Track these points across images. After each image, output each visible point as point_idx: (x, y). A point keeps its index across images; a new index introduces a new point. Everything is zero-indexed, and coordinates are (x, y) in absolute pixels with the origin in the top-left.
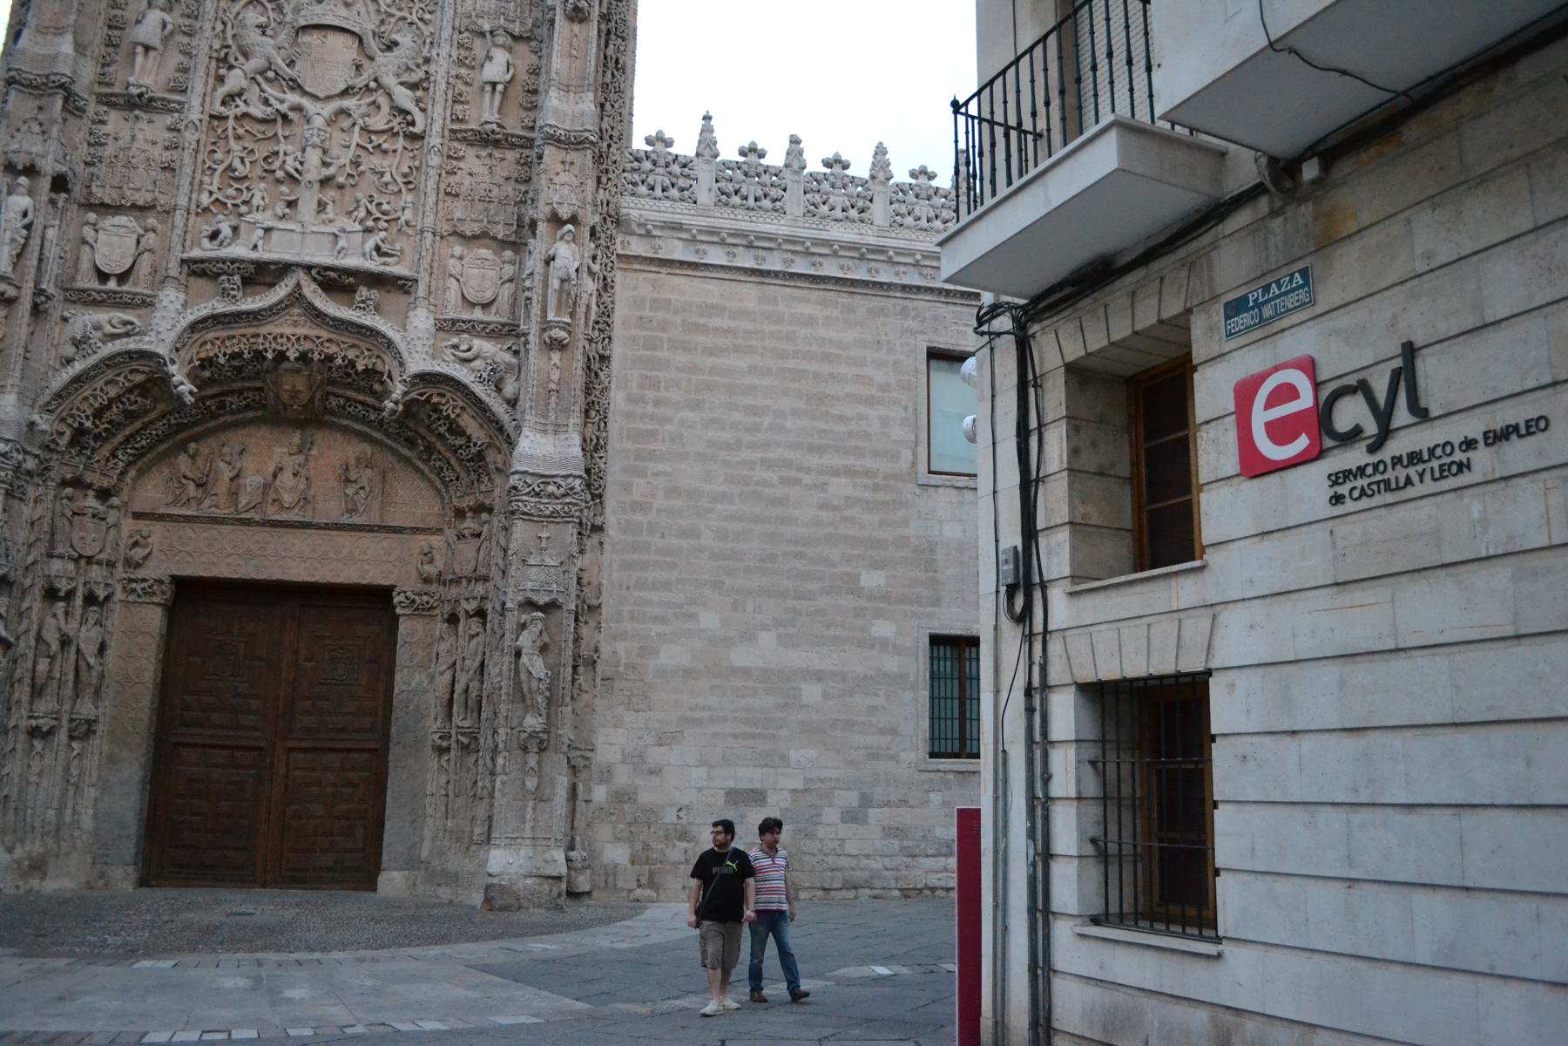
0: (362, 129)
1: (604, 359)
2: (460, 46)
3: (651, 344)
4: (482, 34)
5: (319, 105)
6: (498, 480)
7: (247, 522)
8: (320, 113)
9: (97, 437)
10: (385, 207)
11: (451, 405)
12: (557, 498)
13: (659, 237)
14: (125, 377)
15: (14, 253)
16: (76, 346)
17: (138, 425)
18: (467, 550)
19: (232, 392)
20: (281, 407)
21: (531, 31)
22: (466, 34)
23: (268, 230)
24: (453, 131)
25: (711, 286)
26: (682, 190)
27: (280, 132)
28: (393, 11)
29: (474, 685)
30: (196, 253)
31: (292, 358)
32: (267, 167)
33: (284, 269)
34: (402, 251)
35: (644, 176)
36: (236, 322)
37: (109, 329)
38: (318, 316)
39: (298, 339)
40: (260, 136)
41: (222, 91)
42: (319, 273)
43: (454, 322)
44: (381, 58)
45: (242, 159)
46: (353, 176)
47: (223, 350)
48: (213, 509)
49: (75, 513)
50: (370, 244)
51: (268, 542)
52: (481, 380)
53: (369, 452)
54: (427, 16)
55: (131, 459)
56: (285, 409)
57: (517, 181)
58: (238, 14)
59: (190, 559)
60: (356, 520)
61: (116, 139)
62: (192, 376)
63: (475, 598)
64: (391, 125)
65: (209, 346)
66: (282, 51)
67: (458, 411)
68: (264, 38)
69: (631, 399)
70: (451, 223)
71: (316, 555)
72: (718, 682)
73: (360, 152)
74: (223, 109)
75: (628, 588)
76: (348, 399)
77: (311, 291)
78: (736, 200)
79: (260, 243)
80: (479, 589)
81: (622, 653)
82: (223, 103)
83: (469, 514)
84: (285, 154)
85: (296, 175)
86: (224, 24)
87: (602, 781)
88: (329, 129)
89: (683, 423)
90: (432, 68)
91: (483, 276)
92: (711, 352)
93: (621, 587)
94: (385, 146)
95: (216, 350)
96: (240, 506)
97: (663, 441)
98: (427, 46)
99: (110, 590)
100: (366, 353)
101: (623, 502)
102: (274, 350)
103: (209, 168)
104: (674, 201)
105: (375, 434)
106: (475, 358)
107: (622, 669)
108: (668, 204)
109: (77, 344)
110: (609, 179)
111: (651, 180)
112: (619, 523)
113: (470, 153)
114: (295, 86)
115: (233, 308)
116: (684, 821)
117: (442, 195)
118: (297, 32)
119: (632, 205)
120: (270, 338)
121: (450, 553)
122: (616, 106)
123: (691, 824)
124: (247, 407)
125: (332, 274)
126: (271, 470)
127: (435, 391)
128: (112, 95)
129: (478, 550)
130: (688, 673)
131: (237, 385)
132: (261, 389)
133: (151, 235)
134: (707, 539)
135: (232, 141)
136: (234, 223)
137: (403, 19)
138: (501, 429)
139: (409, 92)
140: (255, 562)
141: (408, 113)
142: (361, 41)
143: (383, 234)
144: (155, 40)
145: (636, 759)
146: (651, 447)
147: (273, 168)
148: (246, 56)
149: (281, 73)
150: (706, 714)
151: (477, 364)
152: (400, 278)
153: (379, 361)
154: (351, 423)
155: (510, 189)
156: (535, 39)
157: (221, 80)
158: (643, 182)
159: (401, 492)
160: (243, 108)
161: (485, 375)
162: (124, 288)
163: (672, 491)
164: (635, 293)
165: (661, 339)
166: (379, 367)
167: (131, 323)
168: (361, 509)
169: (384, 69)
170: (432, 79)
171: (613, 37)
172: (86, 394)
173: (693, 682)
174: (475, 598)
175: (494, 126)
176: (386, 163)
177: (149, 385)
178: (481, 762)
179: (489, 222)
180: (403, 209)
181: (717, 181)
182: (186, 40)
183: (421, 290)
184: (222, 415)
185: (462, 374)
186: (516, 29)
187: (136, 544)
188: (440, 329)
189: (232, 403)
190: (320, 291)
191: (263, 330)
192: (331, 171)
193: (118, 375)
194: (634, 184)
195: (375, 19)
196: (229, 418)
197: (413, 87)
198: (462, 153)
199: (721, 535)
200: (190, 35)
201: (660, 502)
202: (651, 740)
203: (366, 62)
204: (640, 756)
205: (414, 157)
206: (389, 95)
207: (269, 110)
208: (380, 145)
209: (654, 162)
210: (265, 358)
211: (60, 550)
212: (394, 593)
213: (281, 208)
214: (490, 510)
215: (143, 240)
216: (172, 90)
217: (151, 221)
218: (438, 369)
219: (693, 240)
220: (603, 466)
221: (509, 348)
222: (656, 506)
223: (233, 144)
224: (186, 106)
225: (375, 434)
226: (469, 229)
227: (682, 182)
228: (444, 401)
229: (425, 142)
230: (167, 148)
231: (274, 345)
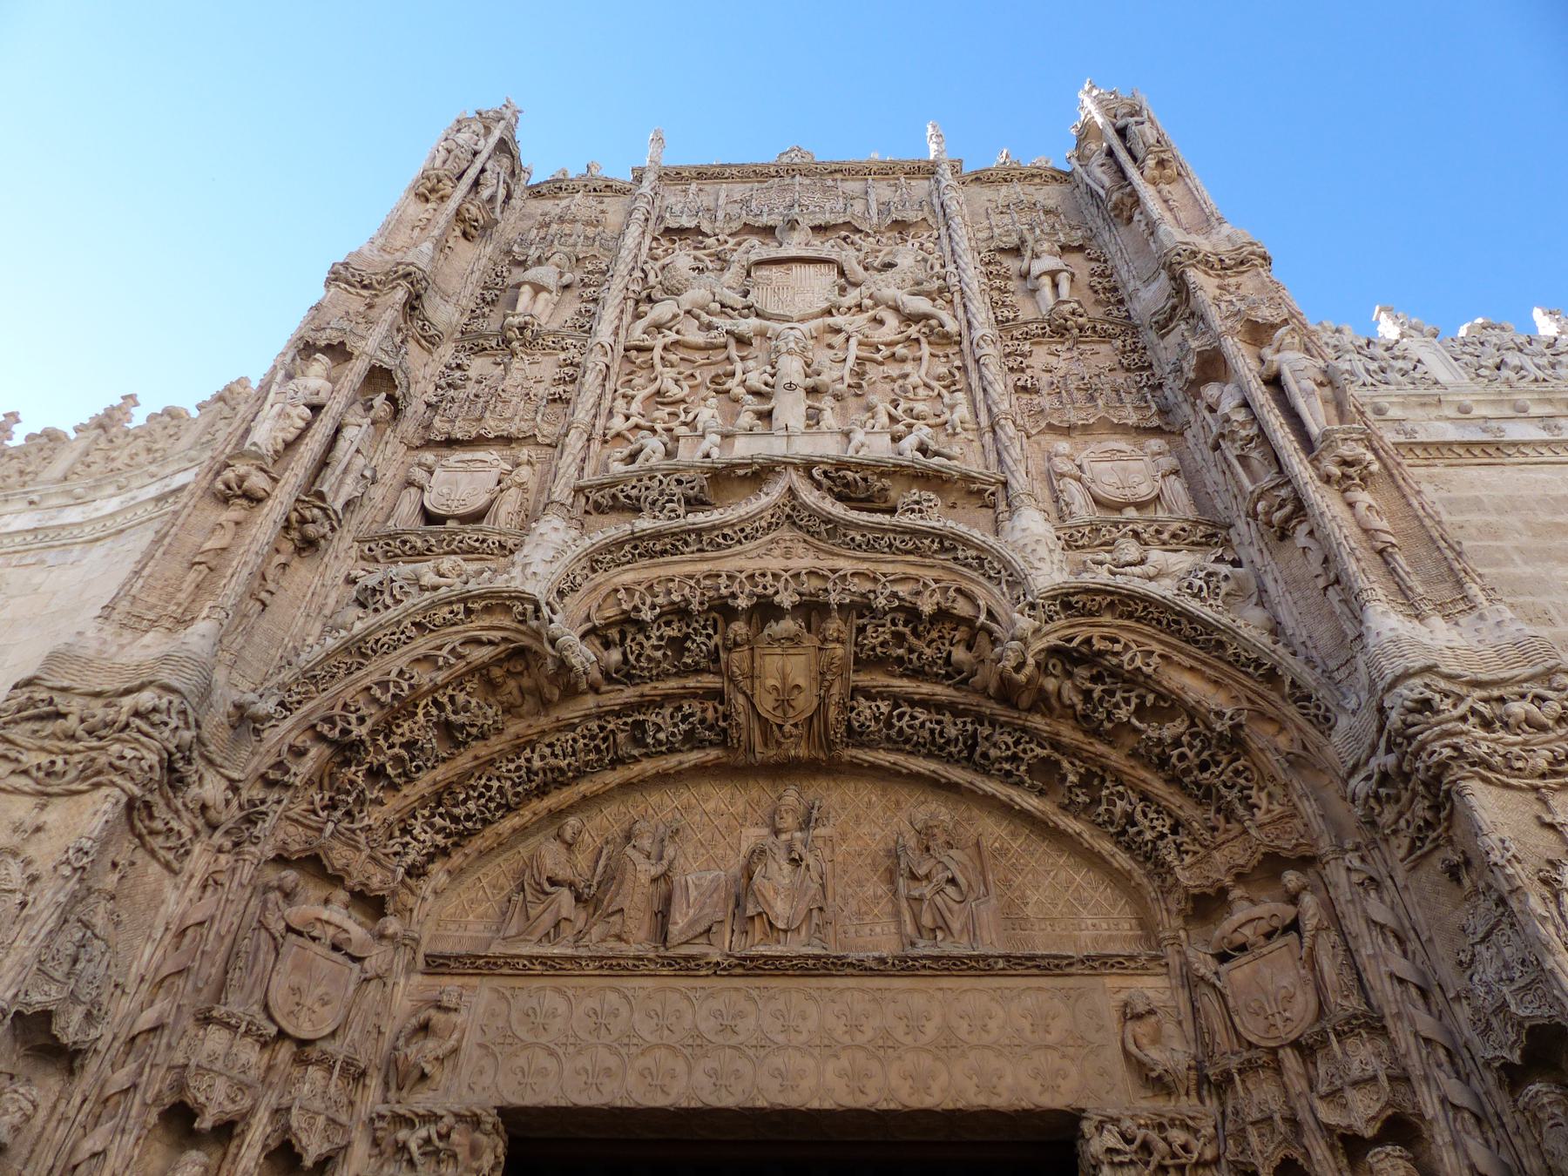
0: (860, 344)
7: (687, 966)
9: (376, 773)
12: (1543, 728)
15: (281, 435)
17: (464, 761)
20: (757, 737)
36: (676, 550)
42: (825, 473)
47: (649, 601)
48: (612, 943)
51: (741, 1015)
53: (947, 818)
55: (440, 839)
59: (551, 1064)
60: (948, 948)
67: (1155, 660)
71: (861, 1039)
76: (897, 700)
83: (1236, 893)
95: (637, 600)
99: (339, 1140)
100: (934, 586)
105: (958, 775)
121: (1209, 1002)
124: (692, 740)
127: (1096, 632)
129: (1312, 962)
131: (672, 685)
132: (717, 695)
138: (1272, 676)
140: (709, 1064)
154: (900, 759)
159: (1033, 897)
166: (962, 608)
168: (956, 926)
172: (367, 682)
184: (636, 760)
187: (425, 1028)
189: (659, 729)
193: (440, 648)
196: (649, 766)
212: (1087, 1127)
225: (958, 775)
228: (1118, 647)
229: (966, 344)
231: (747, 588)
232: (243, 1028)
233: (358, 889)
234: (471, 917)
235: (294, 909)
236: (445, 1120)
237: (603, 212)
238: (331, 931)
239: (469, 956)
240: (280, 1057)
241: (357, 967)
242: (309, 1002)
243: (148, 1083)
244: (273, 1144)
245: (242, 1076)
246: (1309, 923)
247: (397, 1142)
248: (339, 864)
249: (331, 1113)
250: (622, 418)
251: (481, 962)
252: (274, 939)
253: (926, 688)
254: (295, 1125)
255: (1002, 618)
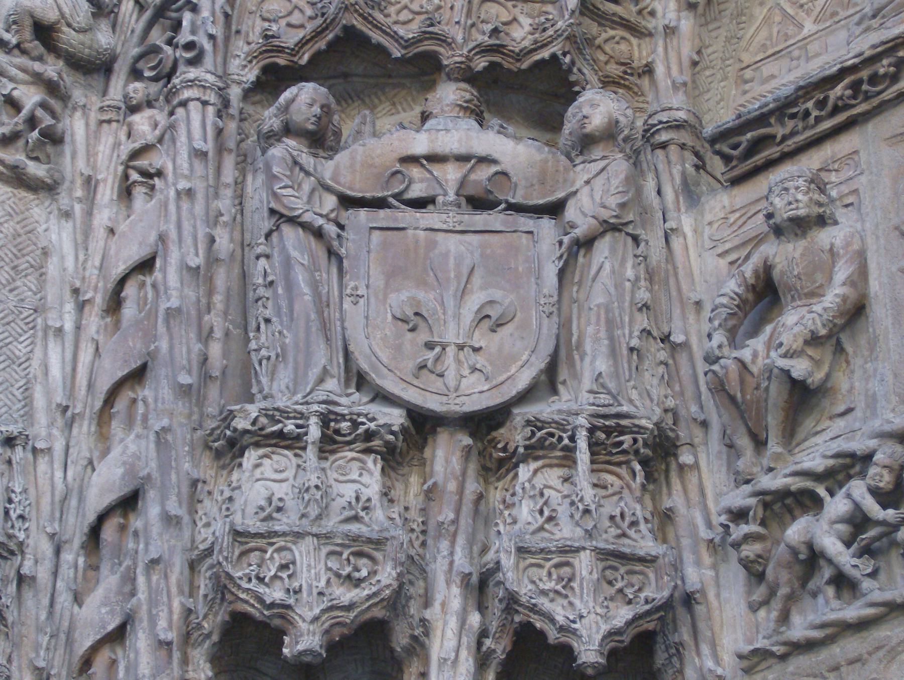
232: (314, 432)
233: (480, 64)
234: (809, 27)
235: (342, 157)
236: (878, 457)
238: (451, 174)
239: (807, 90)
240: (439, 467)
241: (546, 226)
242: (451, 335)
243: (153, 602)
244: (499, 647)
245: (354, 528)
247: (794, 551)
248: (408, 32)
249: (607, 540)
251: (839, 90)
252: (318, 234)
254: (524, 590)
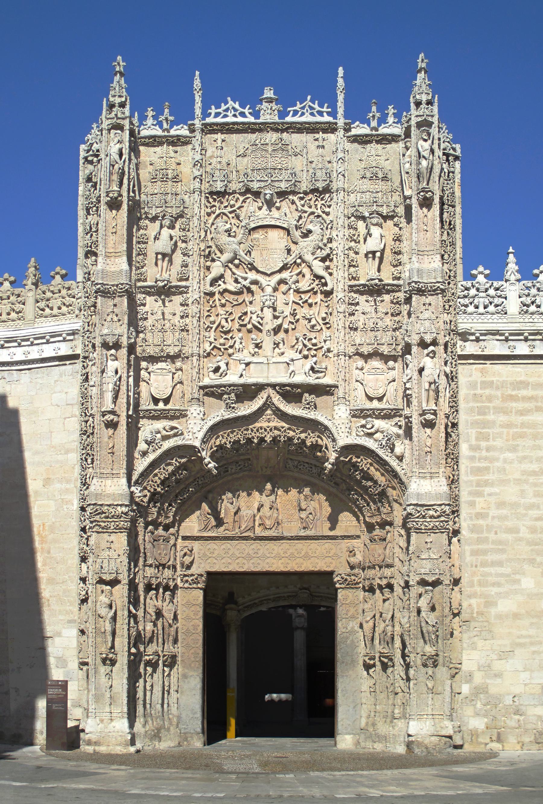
0: (295, 291)
1: (454, 425)
2: (350, 227)
3: (482, 412)
4: (364, 218)
5: (268, 278)
6: (396, 506)
8: (269, 283)
10: (314, 341)
11: (364, 463)
13: (484, 340)
14: (176, 460)
16: (149, 445)
18: (378, 548)
19: (232, 463)
21: (394, 211)
22: (353, 219)
23: (247, 364)
24: (350, 286)
25: (519, 369)
26: (496, 306)
27: (247, 300)
28: (306, 208)
29: (389, 628)
30: (206, 381)
31: (268, 441)
32: (242, 323)
33: (260, 387)
34: (326, 368)
35: (471, 300)
36: (235, 422)
37: (164, 433)
38: (282, 415)
39: (271, 430)
40: (235, 303)
41: (210, 277)
42: (280, 389)
43: (362, 410)
44: (303, 243)
45: (226, 319)
46: (292, 323)
47: (229, 439)
49: (155, 540)
50: (308, 367)
52: (382, 447)
54: (327, 210)
56: (262, 470)
57: (392, 315)
58: (213, 224)
61: (152, 314)
62: (212, 457)
63: (385, 578)
64: (312, 286)
65: (221, 438)
66: (242, 245)
67: (368, 466)
68: (232, 239)
69: (472, 448)
70: (355, 347)
72: (535, 620)
73: (295, 306)
74: (212, 289)
75: (476, 566)
76: (299, 462)
77: (277, 400)
78: (533, 308)
79: (244, 373)
80: (387, 572)
81: (475, 606)
82: (211, 285)
84: (251, 313)
85: (260, 326)
86: (206, 232)
87: (467, 682)
88: (275, 294)
89: (505, 461)
90: (334, 245)
91: (377, 380)
92: (521, 413)
93: (472, 566)
94: (310, 301)
96: (242, 529)
97: (493, 473)
98: (329, 230)
101: (470, 513)
102: (258, 437)
103: (208, 327)
104: (493, 314)
106: (376, 432)
107: (475, 615)
108: (489, 316)
109: (148, 443)
110: (450, 306)
111: (476, 301)
112: (469, 527)
113: (362, 299)
114: (252, 268)
115: (233, 415)
116: (517, 704)
117: (348, 330)
118: (250, 231)
119: (465, 321)
120: (255, 430)
122: (451, 255)
123: (522, 705)
125: (288, 388)
126: (256, 505)
128: (147, 287)
129: (385, 548)
130: (516, 616)
132: (249, 459)
133: (180, 373)
134: (524, 533)
135: (219, 308)
136: (226, 361)
137: (313, 213)
138: (395, 475)
139: (321, 264)
141: (323, 278)
142: (289, 234)
143: (315, 359)
144: (169, 251)
145: (486, 668)
146: (486, 478)
147: (245, 323)
148: (221, 252)
149: (243, 260)
150: (528, 640)
151: (378, 436)
152: (328, 386)
153: (319, 439)
155: (389, 320)
156: (397, 216)
157: (208, 268)
158: (471, 303)
160: (223, 286)
161: (384, 443)
162: (168, 407)
163: (501, 505)
164: (470, 379)
165: (488, 408)
166: (320, 442)
167: (176, 428)
169: (305, 250)
170: (334, 252)
171: (446, 207)
173: (519, 621)
174: (385, 578)
175: (377, 281)
176: (311, 312)
177: (189, 464)
178: (396, 672)
179: (378, 344)
180: (325, 341)
181: (520, 297)
182: (184, 245)
183: (340, 392)
185: (370, 443)
186: (385, 211)
188: (354, 416)
189: (232, 469)
190: (281, 399)
191: (251, 427)
192: (279, 321)
194: (466, 306)
195: (296, 215)
196: (230, 478)
197: (323, 260)
198: (357, 301)
199: (533, 530)
200: (186, 242)
201: (493, 512)
202: (495, 657)
203: (293, 247)
204: (489, 666)
205: (327, 306)
206: (310, 267)
207: (239, 285)
208: (306, 301)
209: (478, 290)
210: (253, 442)
211: (150, 561)
213: (251, 348)
214: (391, 524)
215: (176, 376)
216: (181, 280)
217: (179, 364)
218: (356, 442)
219: (507, 340)
220: (457, 493)
221: (397, 424)
222: (491, 514)
223: (221, 311)
224: (190, 289)
226: (366, 350)
227: (497, 301)
228: (359, 460)
229: (334, 295)
230: (182, 317)
231: (258, 434)
237: (179, 164)
246: (387, 541)
250: (209, 344)
253: (307, 460)
255: (329, 449)
